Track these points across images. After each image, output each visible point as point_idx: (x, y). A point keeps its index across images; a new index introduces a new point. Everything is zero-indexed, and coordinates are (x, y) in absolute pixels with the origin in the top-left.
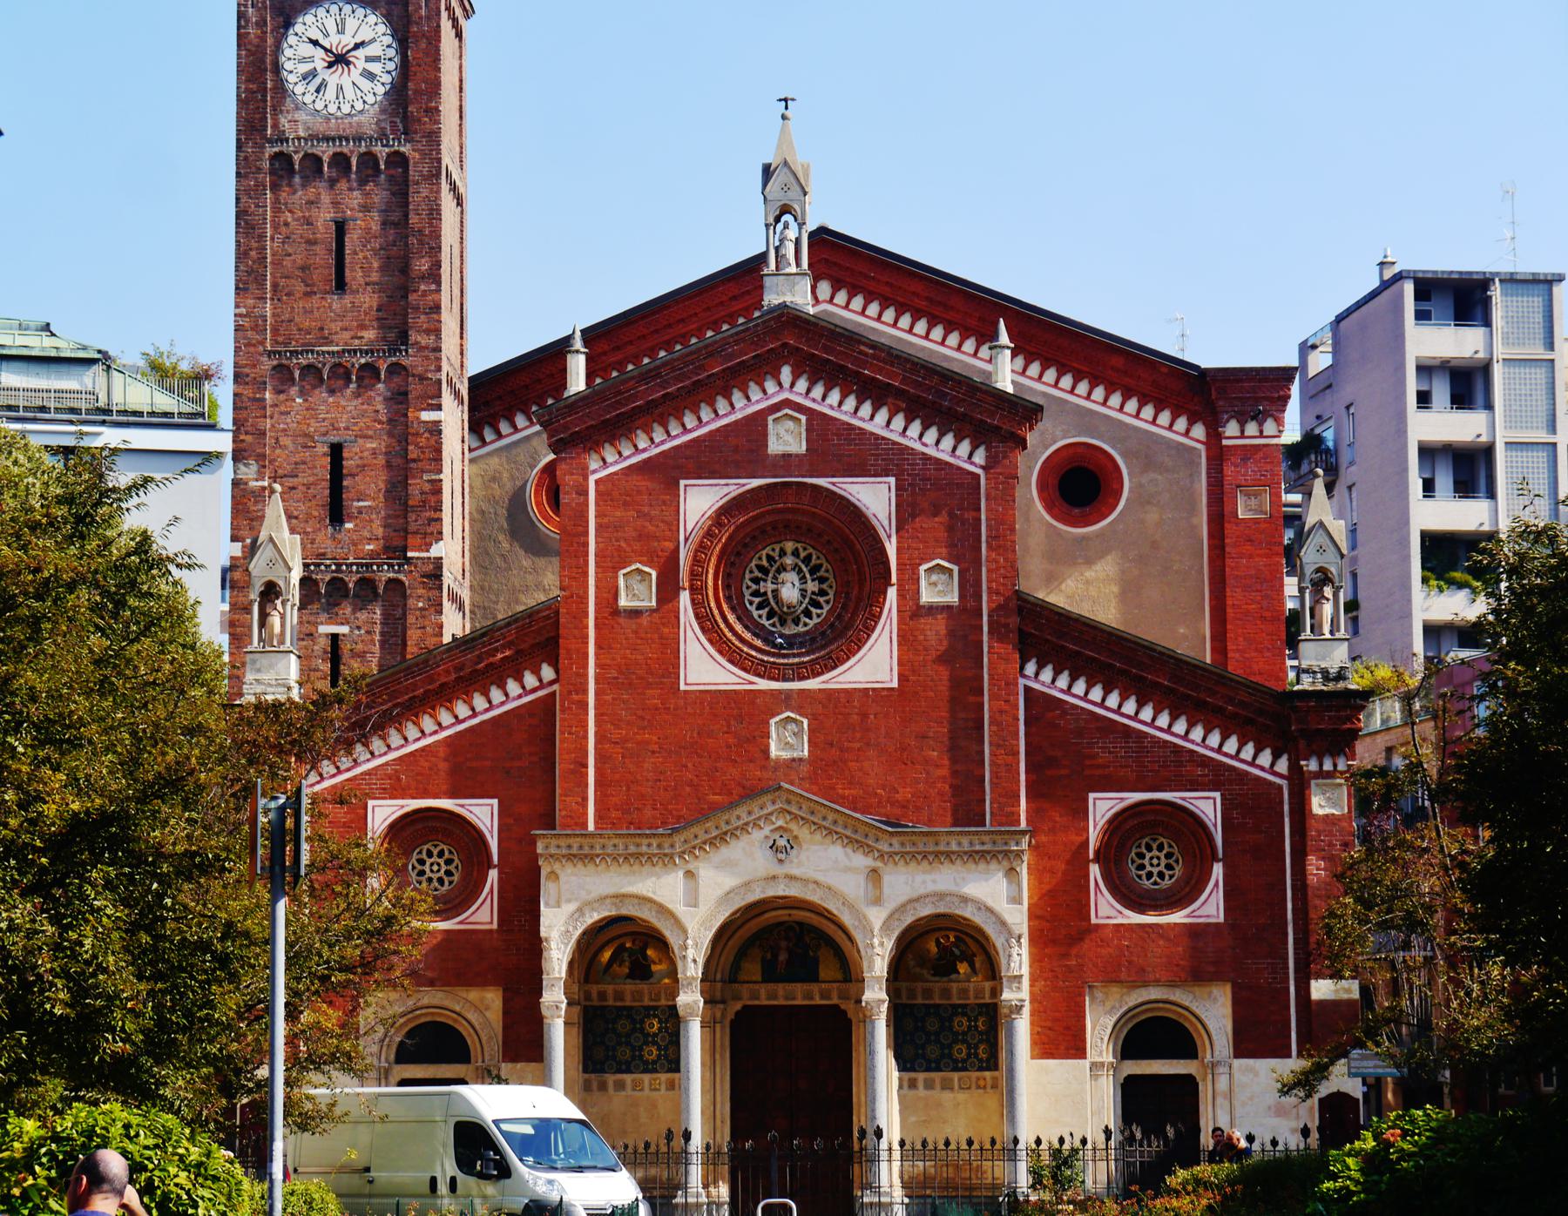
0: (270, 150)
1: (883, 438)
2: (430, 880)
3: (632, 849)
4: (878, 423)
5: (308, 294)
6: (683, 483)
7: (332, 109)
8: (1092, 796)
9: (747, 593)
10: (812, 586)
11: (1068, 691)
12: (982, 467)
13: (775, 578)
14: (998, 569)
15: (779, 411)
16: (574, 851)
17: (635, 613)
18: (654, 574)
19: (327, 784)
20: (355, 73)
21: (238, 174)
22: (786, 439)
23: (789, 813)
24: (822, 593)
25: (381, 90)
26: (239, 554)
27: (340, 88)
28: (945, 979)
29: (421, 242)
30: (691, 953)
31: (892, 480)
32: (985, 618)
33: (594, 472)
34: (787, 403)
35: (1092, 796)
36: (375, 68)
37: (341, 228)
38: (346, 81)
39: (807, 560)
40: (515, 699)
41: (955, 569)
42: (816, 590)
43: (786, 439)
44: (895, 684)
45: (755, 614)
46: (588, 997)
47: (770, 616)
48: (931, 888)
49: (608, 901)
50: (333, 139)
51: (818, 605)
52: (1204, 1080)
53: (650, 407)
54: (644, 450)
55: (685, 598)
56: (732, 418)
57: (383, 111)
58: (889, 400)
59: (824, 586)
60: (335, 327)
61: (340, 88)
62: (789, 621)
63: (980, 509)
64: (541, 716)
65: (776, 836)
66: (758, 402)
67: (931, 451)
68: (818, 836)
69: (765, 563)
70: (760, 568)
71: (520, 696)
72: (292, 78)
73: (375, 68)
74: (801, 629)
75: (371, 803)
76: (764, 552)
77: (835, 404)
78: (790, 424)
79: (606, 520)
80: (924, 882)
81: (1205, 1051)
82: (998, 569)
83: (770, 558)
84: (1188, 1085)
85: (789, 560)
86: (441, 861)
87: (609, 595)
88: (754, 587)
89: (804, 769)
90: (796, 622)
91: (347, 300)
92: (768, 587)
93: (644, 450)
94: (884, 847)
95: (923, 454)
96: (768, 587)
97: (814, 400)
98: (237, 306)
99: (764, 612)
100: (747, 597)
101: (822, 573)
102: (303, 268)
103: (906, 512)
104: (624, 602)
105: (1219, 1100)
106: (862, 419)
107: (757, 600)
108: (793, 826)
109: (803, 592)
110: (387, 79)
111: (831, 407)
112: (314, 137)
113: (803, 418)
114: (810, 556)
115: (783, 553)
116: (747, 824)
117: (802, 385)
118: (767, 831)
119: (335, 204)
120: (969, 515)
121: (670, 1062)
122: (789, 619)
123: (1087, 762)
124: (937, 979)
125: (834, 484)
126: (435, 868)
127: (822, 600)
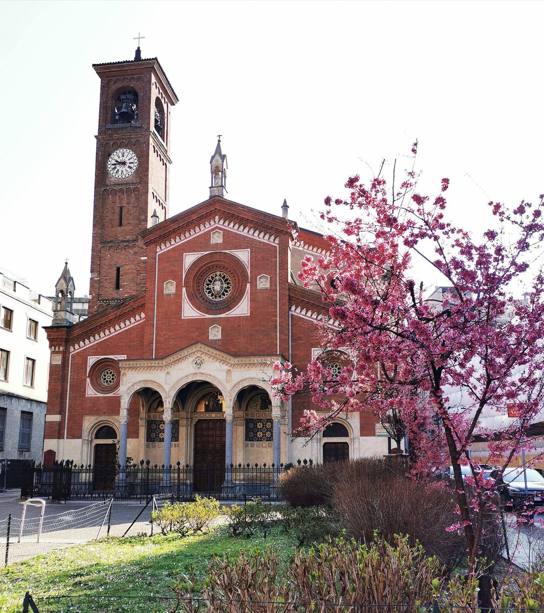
0: (103, 189)
1: (247, 237)
2: (107, 381)
3: (149, 365)
4: (245, 232)
5: (113, 227)
6: (184, 254)
7: (120, 177)
8: (313, 349)
9: (205, 289)
10: (225, 286)
11: (305, 315)
12: (278, 244)
13: (214, 283)
14: (282, 276)
15: (214, 230)
16: (131, 366)
17: (169, 295)
18: (175, 283)
19: (76, 352)
20: (126, 167)
21: (95, 196)
22: (217, 239)
23: (201, 351)
24: (228, 287)
25: (133, 171)
26: (91, 298)
27: (122, 171)
28: (264, 410)
29: (142, 211)
30: (168, 400)
31: (249, 250)
32: (278, 292)
33: (158, 252)
34: (217, 228)
35: (313, 349)
36: (131, 165)
37: (121, 209)
38: (124, 170)
39: (224, 277)
40: (133, 324)
41: (269, 277)
42: (226, 287)
43: (217, 239)
44: (249, 315)
45: (207, 295)
46: (149, 417)
47: (212, 295)
48: (248, 376)
49: (142, 383)
50: (120, 184)
51: (227, 292)
52: (351, 444)
53: (174, 231)
54: (173, 245)
55: (184, 289)
56: (200, 233)
57: (134, 177)
58: (249, 224)
59: (229, 285)
60: (119, 235)
61: (122, 171)
62: (218, 297)
63: (277, 258)
64: (141, 329)
65: (197, 359)
66: (208, 228)
67: (262, 240)
68: (211, 359)
69: (211, 279)
70: (209, 281)
71: (134, 323)
72: (110, 169)
73: (131, 165)
74: (221, 299)
75: (89, 357)
76: (210, 276)
77: (232, 227)
78: (217, 234)
79: (161, 267)
80: (246, 374)
81: (351, 434)
82: (282, 276)
83: (212, 277)
84: (345, 446)
85: (217, 278)
86: (111, 375)
87: (161, 289)
88: (207, 287)
89: (220, 343)
90: (220, 297)
91: (122, 228)
92: (211, 286)
93: (173, 245)
94: (233, 362)
95: (259, 241)
96: (211, 286)
97: (225, 226)
98: (93, 231)
99: (210, 295)
100: (205, 290)
101: (228, 281)
102: (110, 220)
103: (253, 258)
104: (166, 292)
105: (355, 451)
106: (240, 231)
107: (208, 291)
108: (203, 356)
109: (222, 287)
110: (135, 168)
111: (231, 228)
112: (115, 184)
113: (222, 232)
114: (224, 277)
115: (216, 275)
116: (187, 355)
117: (222, 222)
118: (194, 358)
119: (120, 202)
120: (273, 260)
121: (175, 438)
122: (218, 296)
123: (311, 338)
124: (262, 410)
125: (231, 252)
126: (109, 377)
127: (228, 290)
